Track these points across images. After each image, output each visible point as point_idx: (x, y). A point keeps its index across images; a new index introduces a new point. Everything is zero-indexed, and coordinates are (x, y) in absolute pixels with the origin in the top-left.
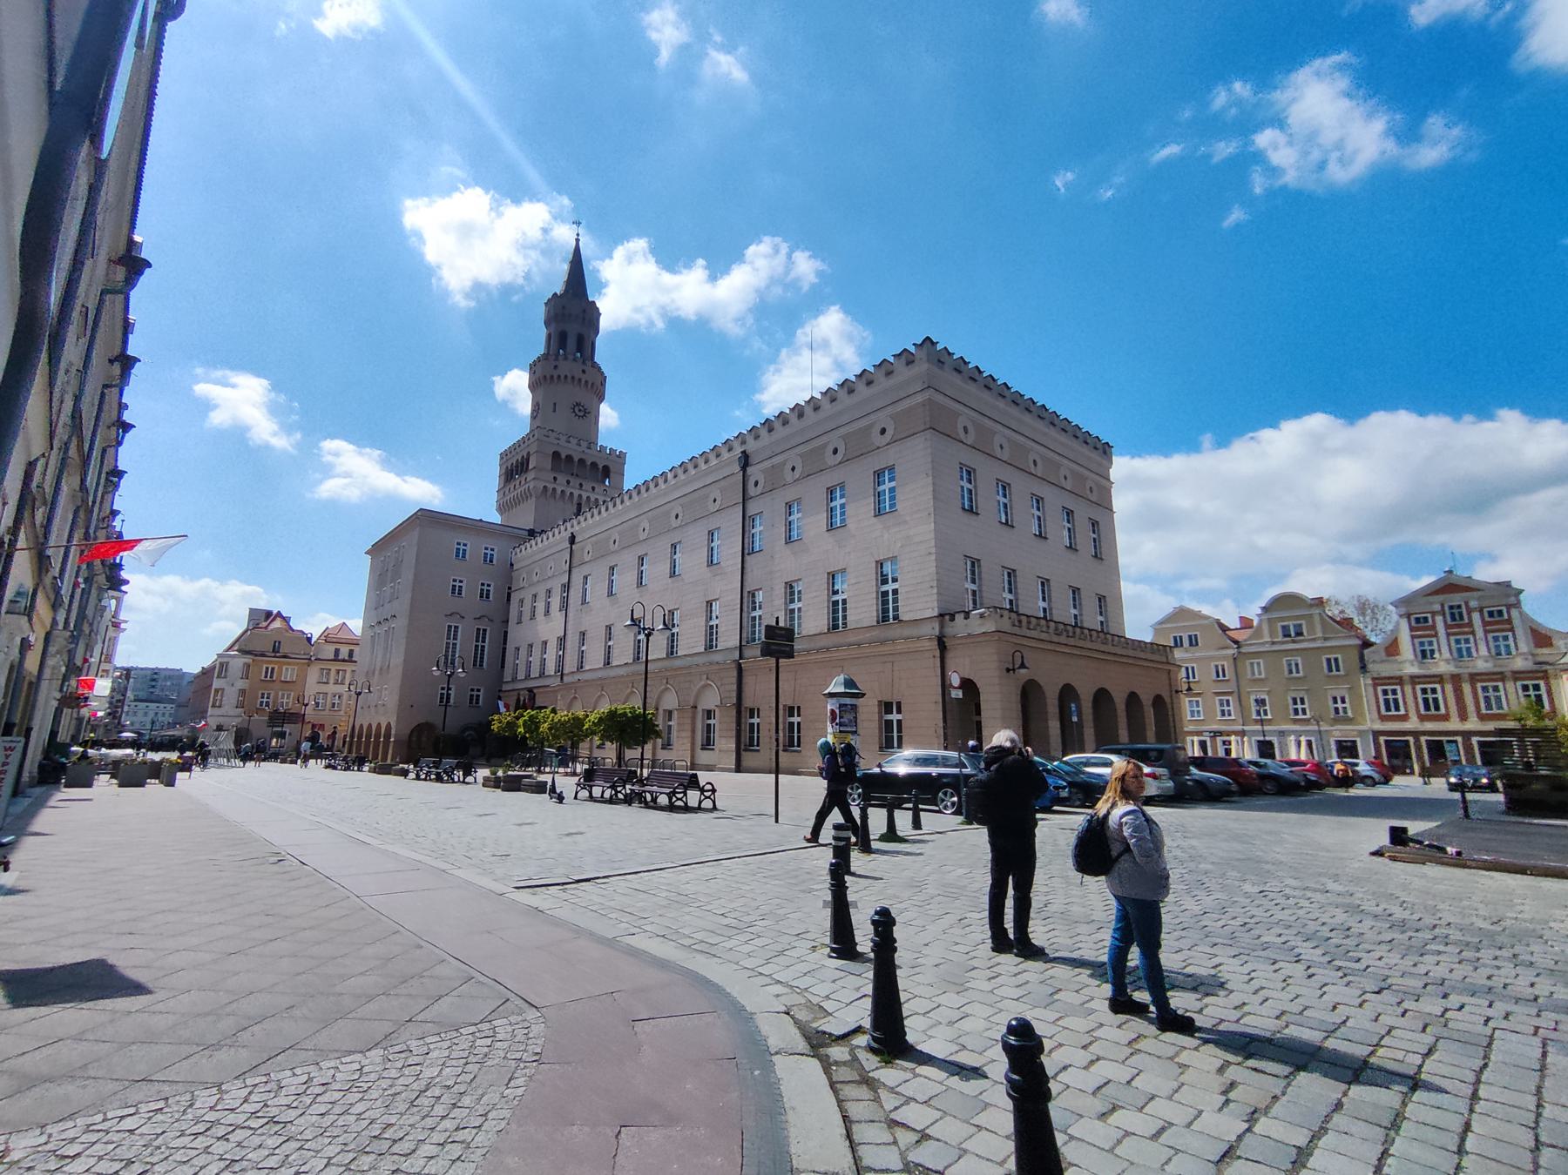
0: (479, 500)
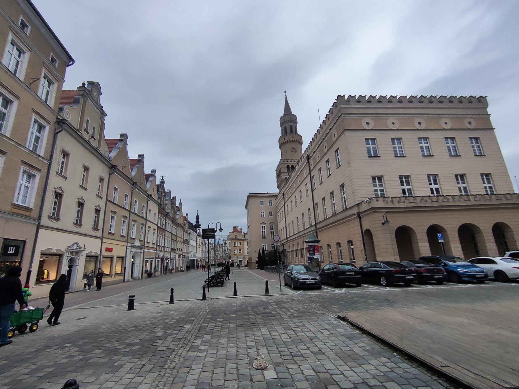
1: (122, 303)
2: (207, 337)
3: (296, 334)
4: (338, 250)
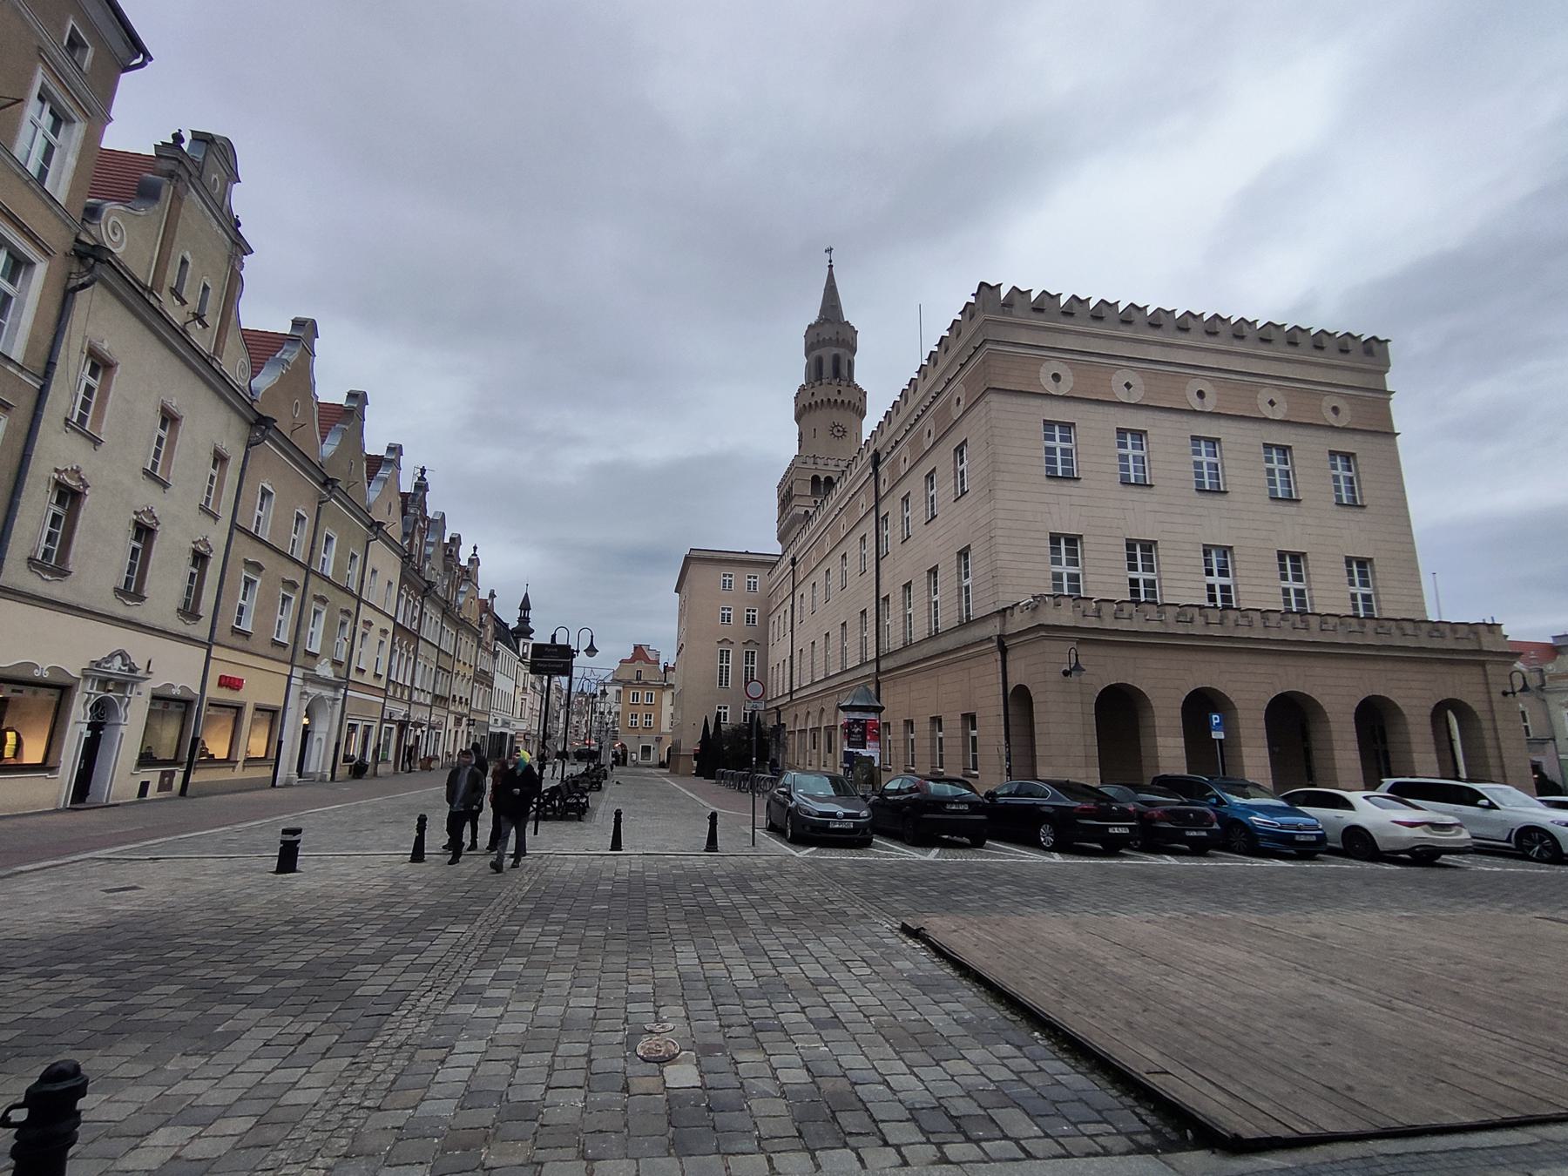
0: (757, 531)
1: (257, 851)
2: (514, 964)
3: (775, 967)
4: (933, 739)
